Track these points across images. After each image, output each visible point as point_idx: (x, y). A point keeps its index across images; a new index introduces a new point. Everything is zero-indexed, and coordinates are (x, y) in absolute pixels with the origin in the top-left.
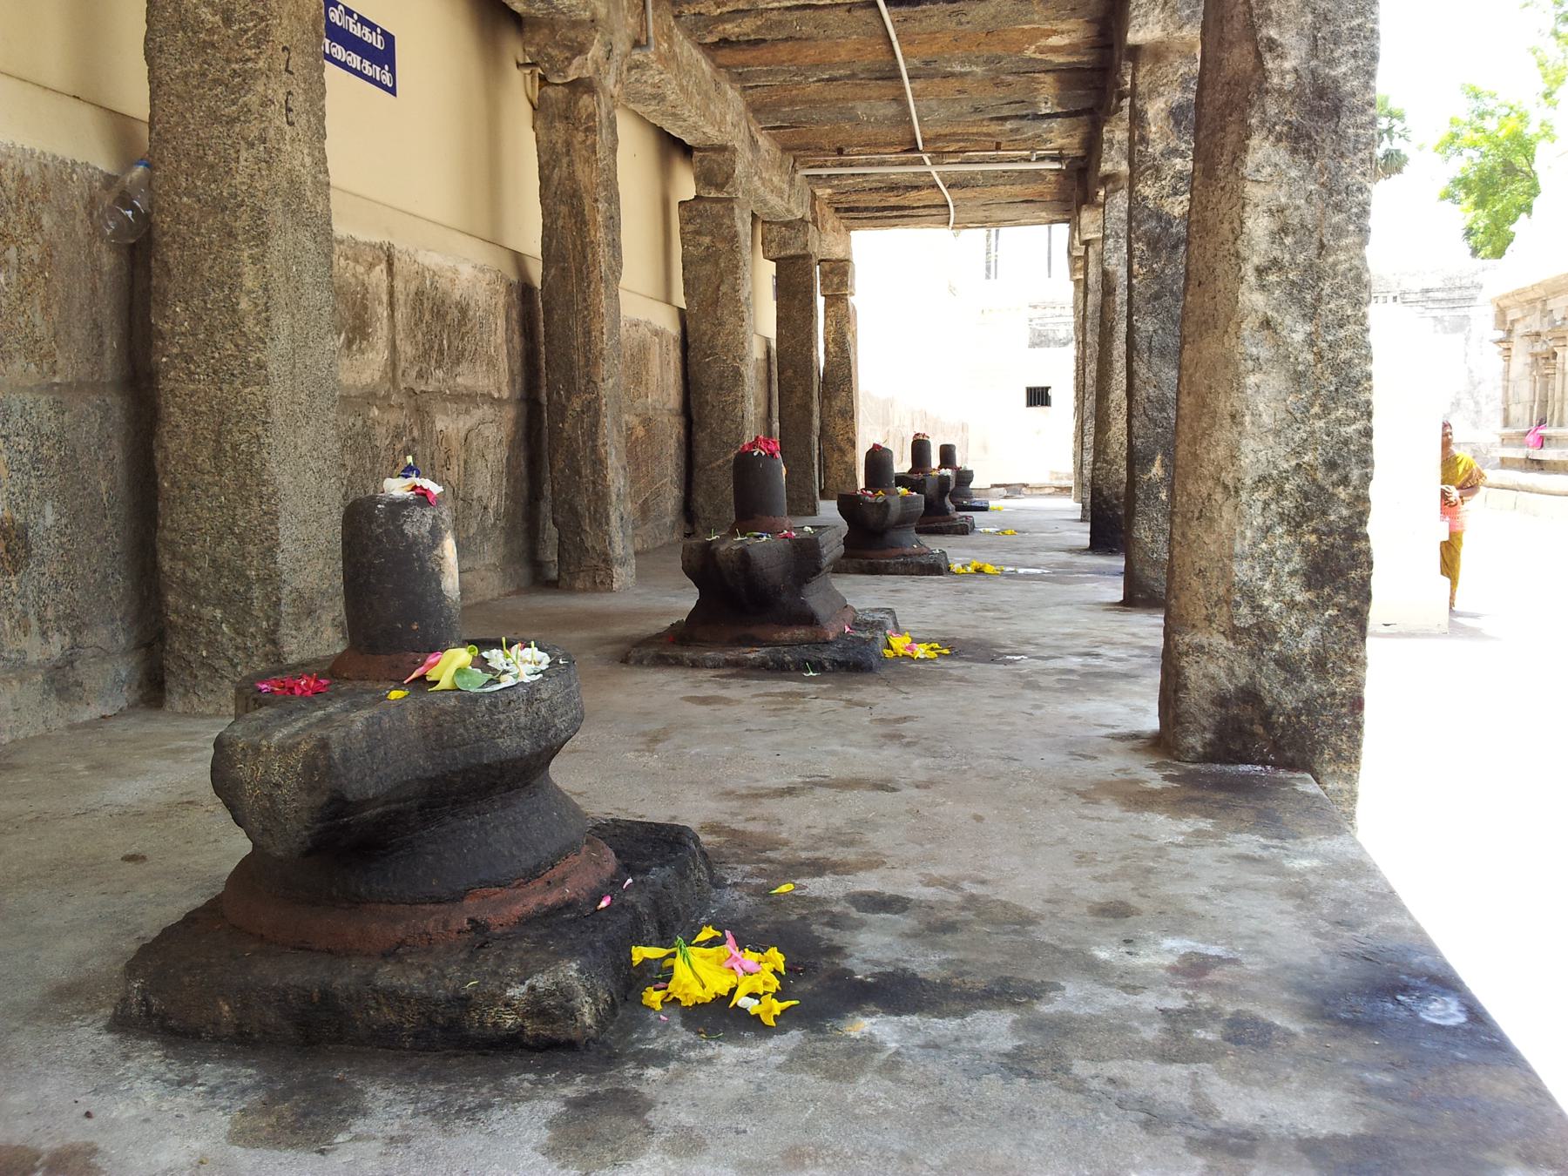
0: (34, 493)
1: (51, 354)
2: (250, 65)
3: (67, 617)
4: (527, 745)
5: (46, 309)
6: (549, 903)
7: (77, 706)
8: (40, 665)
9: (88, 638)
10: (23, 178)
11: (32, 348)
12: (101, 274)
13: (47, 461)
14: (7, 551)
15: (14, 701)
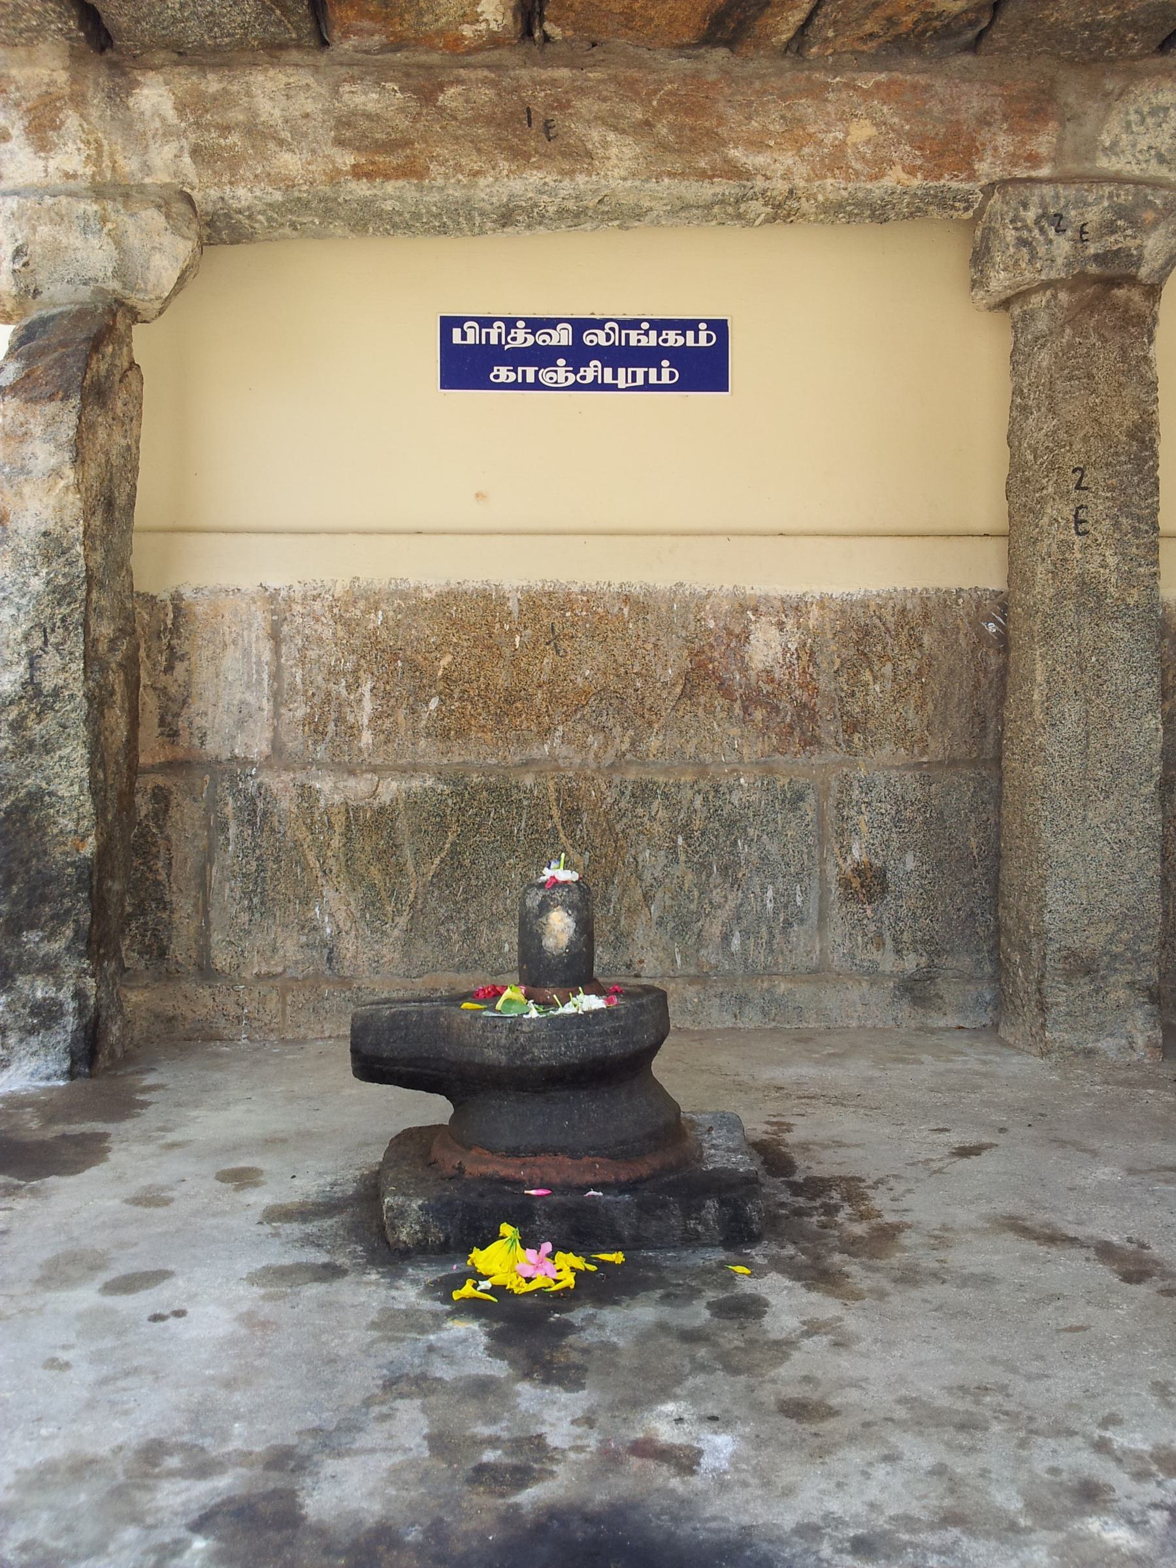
3: (924, 942)
4: (504, 1059)
5: (920, 707)
7: (933, 1014)
8: (892, 975)
9: (948, 961)
10: (904, 610)
11: (903, 735)
12: (986, 672)
13: (912, 821)
14: (862, 886)
15: (862, 997)
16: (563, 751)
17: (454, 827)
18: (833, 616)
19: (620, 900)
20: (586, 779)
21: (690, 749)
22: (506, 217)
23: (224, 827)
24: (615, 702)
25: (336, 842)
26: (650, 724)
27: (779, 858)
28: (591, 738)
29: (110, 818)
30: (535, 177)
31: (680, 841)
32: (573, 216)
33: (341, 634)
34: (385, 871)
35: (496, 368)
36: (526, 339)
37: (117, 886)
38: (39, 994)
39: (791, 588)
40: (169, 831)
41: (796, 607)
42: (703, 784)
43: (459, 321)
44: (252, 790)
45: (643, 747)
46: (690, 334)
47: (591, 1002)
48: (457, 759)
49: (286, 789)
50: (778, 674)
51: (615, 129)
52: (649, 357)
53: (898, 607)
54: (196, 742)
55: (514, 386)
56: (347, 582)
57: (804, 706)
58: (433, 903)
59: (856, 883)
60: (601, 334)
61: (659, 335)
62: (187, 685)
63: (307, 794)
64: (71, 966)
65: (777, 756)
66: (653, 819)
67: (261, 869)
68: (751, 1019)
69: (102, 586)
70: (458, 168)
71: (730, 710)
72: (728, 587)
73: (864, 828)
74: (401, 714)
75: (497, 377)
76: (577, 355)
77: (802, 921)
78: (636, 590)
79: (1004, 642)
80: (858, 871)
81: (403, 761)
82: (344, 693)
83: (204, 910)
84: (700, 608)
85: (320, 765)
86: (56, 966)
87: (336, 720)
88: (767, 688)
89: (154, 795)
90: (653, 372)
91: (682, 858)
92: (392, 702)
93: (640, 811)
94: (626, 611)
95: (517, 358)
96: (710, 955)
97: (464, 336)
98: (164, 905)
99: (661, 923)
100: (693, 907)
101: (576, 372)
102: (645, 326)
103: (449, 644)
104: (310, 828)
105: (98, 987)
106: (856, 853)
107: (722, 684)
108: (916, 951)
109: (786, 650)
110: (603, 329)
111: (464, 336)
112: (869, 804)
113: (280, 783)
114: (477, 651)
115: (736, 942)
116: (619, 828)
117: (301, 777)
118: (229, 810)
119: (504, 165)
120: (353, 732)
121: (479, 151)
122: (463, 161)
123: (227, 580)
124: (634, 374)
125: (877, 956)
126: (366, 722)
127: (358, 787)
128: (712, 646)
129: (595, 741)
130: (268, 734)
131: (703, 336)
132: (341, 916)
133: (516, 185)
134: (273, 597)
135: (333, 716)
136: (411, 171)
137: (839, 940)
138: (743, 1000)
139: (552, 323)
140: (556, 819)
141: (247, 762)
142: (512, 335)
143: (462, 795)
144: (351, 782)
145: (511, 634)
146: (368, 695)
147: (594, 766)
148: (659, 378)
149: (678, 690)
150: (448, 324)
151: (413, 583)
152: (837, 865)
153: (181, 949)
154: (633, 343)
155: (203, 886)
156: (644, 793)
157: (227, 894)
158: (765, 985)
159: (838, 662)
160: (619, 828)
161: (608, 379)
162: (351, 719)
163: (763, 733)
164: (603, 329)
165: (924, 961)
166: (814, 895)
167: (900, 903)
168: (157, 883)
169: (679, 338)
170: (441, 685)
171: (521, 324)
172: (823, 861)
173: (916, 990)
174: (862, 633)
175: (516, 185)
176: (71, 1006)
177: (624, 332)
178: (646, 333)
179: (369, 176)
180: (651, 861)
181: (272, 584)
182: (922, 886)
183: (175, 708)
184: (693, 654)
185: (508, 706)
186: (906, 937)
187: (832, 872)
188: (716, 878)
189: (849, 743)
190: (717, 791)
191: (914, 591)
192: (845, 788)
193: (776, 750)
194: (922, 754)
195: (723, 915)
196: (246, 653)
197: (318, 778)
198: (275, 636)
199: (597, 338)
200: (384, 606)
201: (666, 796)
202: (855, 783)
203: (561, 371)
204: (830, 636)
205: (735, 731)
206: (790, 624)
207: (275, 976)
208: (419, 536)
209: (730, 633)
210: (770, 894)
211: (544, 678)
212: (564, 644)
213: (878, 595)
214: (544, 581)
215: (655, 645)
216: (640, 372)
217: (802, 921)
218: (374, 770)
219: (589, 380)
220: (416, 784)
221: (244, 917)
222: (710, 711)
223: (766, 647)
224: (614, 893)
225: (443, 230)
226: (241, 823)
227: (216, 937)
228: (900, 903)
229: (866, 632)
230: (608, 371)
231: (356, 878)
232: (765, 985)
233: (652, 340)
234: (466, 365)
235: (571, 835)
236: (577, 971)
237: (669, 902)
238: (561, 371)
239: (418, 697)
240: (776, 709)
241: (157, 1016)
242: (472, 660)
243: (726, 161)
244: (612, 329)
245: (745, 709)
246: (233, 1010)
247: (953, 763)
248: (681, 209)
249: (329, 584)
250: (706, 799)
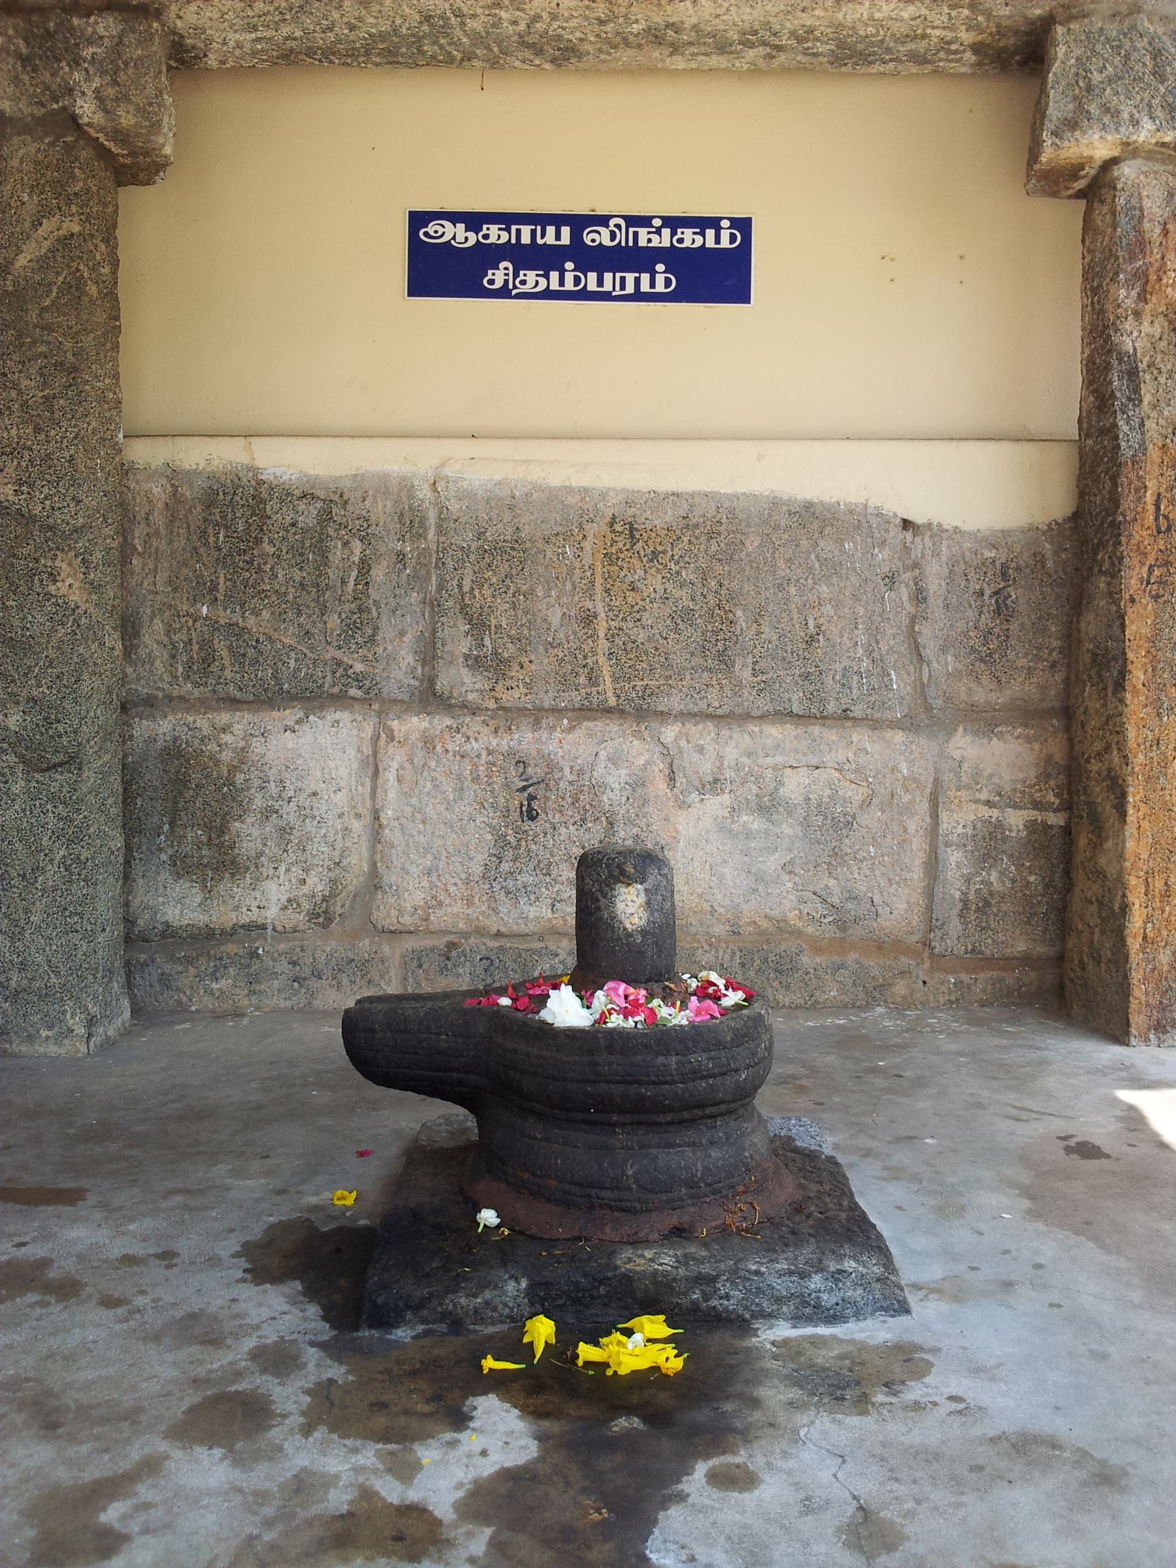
46: (710, 233)
60: (605, 232)
61: (673, 234)
110: (607, 226)
131: (725, 235)
154: (642, 242)
164: (607, 226)
169: (696, 237)
177: (631, 230)
178: (658, 232)
199: (603, 237)
233: (664, 240)
244: (618, 226)
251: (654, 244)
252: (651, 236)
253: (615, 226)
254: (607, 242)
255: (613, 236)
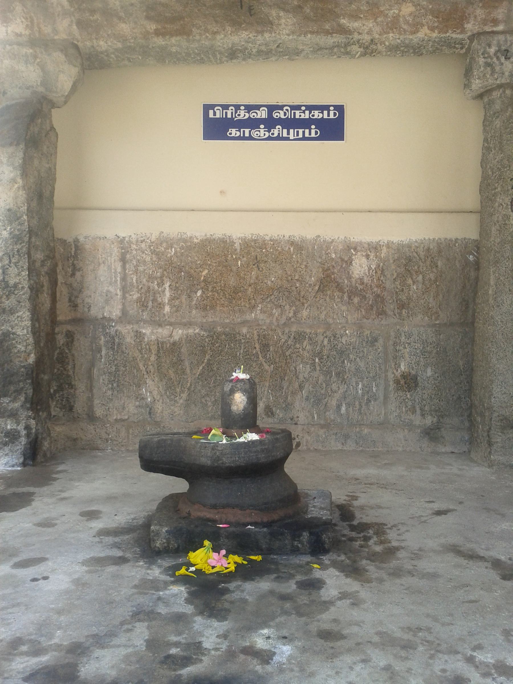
0: (422, 363)
1: (437, 313)
2: (496, 190)
6: (208, 516)
8: (419, 426)
10: (428, 250)
13: (430, 353)
14: (405, 383)
16: (261, 316)
17: (209, 352)
18: (393, 252)
19: (288, 388)
20: (272, 330)
21: (322, 316)
22: (233, 54)
23: (100, 351)
24: (286, 293)
25: (153, 358)
26: (303, 304)
27: (365, 369)
28: (274, 311)
29: (42, 345)
30: (244, 35)
31: (317, 360)
32: (265, 54)
33: (154, 259)
34: (176, 372)
35: (230, 130)
36: (245, 115)
37: (46, 377)
38: (9, 427)
39: (373, 238)
40: (74, 352)
41: (375, 247)
42: (329, 333)
43: (212, 107)
44: (113, 333)
45: (299, 315)
46: (325, 112)
47: (253, 437)
48: (210, 320)
49: (129, 333)
50: (366, 280)
51: (284, 10)
52: (305, 124)
53: (426, 247)
54: (86, 310)
55: (239, 138)
56: (158, 234)
57: (378, 296)
58: (199, 388)
59: (402, 382)
62: (82, 283)
63: (139, 335)
64: (24, 414)
65: (365, 320)
66: (304, 349)
67: (117, 370)
68: (351, 445)
69: (37, 235)
70: (206, 30)
71: (342, 298)
72: (342, 237)
73: (407, 356)
74: (184, 297)
75: (231, 134)
76: (270, 123)
77: (375, 400)
78: (297, 239)
79: (477, 265)
80: (404, 376)
81: (184, 321)
82: (156, 287)
83: (90, 389)
84: (328, 248)
85: (145, 322)
86: (17, 414)
87: (152, 301)
88: (360, 287)
89: (67, 334)
90: (307, 131)
91: (318, 368)
92: (179, 292)
93: (298, 346)
94: (292, 249)
95: (241, 124)
96: (331, 415)
97: (215, 114)
98: (71, 386)
99: (307, 399)
100: (323, 392)
101: (269, 131)
102: (303, 108)
103: (206, 264)
104: (140, 351)
105: (37, 424)
106: (403, 368)
107: (338, 285)
108: (431, 415)
109: (370, 268)
110: (283, 110)
111: (215, 114)
112: (409, 344)
113: (126, 330)
114: (220, 268)
115: (343, 409)
116: (287, 353)
117: (136, 327)
118: (102, 342)
119: (229, 29)
120: (161, 306)
121: (216, 22)
122: (209, 27)
123: (100, 233)
124: (298, 132)
125: (412, 417)
126: (167, 301)
127: (163, 332)
128: (334, 267)
129: (276, 312)
130: (120, 307)
131: (332, 113)
132: (155, 393)
133: (235, 39)
134: (122, 241)
135: (151, 298)
136: (184, 32)
137: (393, 409)
138: (347, 437)
139: (258, 107)
140: (258, 349)
141: (110, 320)
142: (238, 113)
143: (212, 337)
144: (160, 330)
145: (237, 260)
146: (167, 289)
147: (276, 324)
148: (310, 134)
149: (317, 288)
150: (207, 108)
151: (189, 234)
152: (393, 373)
153: (79, 407)
154: (297, 116)
155: (90, 377)
156: (299, 337)
157: (101, 381)
158: (358, 430)
159: (395, 275)
160: (287, 353)
161: (285, 135)
162: (159, 300)
163: (358, 308)
164: (283, 110)
165: (435, 420)
166: (382, 388)
167: (424, 392)
168: (68, 376)
170: (203, 284)
171: (242, 108)
172: (386, 371)
173: (432, 434)
174: (408, 260)
175: (235, 39)
176: (24, 432)
177: (293, 112)
178: (304, 112)
179: (163, 35)
180: (303, 370)
181: (122, 235)
182: (435, 384)
183: (75, 293)
184: (324, 271)
185: (235, 294)
186: (426, 408)
187: (391, 376)
188: (334, 378)
189: (400, 314)
190: (335, 337)
191: (434, 239)
192: (398, 336)
193: (364, 317)
194: (436, 320)
195: (337, 396)
196: (109, 267)
197: (144, 328)
198: (123, 260)
199: (280, 114)
200: (175, 246)
201: (310, 339)
202: (403, 334)
203: (262, 131)
204: (391, 261)
205: (344, 308)
206: (372, 255)
207: (124, 420)
208: (192, 212)
209: (342, 260)
210: (360, 386)
211: (252, 281)
212: (262, 265)
213: (416, 241)
214: (252, 234)
215: (306, 266)
216: (301, 131)
217: (375, 400)
218: (171, 324)
219: (276, 135)
220: (191, 331)
221: (110, 393)
222: (332, 298)
223: (360, 267)
224: (285, 385)
225: (202, 61)
226: (108, 349)
227: (96, 402)
228: (424, 392)
229: (409, 259)
230: (285, 131)
231: (162, 375)
232: (358, 430)
233: (307, 115)
234: (216, 128)
235: (265, 357)
236: (248, 421)
237: (311, 389)
238: (262, 131)
239: (191, 290)
240: (364, 297)
241: (68, 438)
242: (218, 272)
243: (339, 25)
244: (287, 110)
245: (349, 297)
246: (104, 436)
247: (452, 324)
248: (318, 49)
249: (148, 235)
250: (329, 341)
251: (302, 117)
252: (301, 114)
253: (286, 110)
254: (282, 116)
255: (285, 115)
